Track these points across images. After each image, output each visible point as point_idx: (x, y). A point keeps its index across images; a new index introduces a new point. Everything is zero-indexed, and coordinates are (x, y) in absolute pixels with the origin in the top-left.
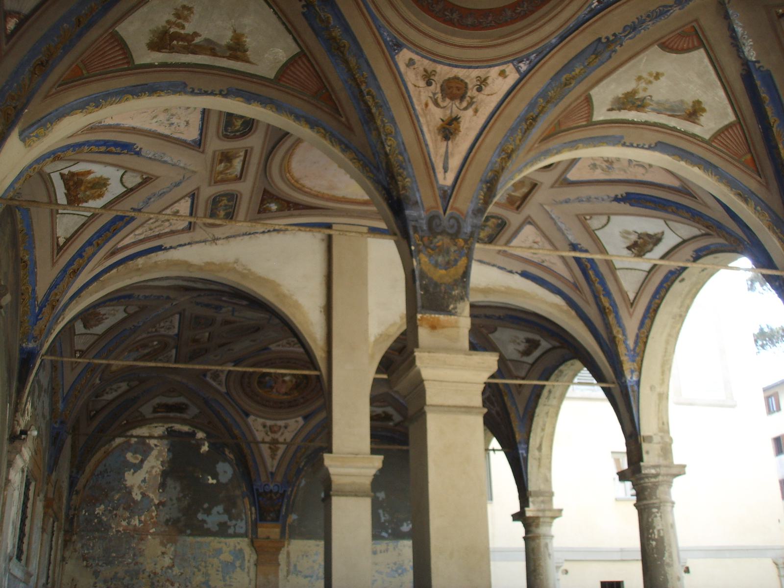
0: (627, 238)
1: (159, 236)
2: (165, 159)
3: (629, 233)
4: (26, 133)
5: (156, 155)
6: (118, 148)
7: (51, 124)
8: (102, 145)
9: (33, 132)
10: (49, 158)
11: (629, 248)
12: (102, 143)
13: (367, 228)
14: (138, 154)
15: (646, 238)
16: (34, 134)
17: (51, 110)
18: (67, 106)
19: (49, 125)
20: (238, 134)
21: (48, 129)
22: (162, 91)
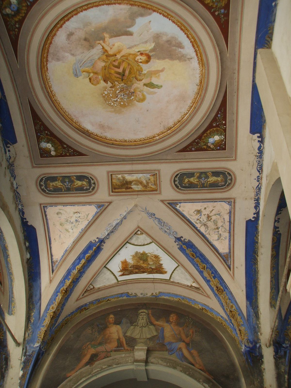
1: (231, 223)
2: (114, 224)
4: (10, 311)
5: (109, 229)
6: (89, 252)
7: (13, 298)
8: (80, 261)
9: (12, 308)
10: (57, 296)
12: (78, 260)
13: (259, 51)
14: (102, 241)
16: (13, 308)
17: (8, 294)
18: (10, 287)
19: (13, 299)
20: (92, 182)
21: (14, 301)
22: (5, 245)
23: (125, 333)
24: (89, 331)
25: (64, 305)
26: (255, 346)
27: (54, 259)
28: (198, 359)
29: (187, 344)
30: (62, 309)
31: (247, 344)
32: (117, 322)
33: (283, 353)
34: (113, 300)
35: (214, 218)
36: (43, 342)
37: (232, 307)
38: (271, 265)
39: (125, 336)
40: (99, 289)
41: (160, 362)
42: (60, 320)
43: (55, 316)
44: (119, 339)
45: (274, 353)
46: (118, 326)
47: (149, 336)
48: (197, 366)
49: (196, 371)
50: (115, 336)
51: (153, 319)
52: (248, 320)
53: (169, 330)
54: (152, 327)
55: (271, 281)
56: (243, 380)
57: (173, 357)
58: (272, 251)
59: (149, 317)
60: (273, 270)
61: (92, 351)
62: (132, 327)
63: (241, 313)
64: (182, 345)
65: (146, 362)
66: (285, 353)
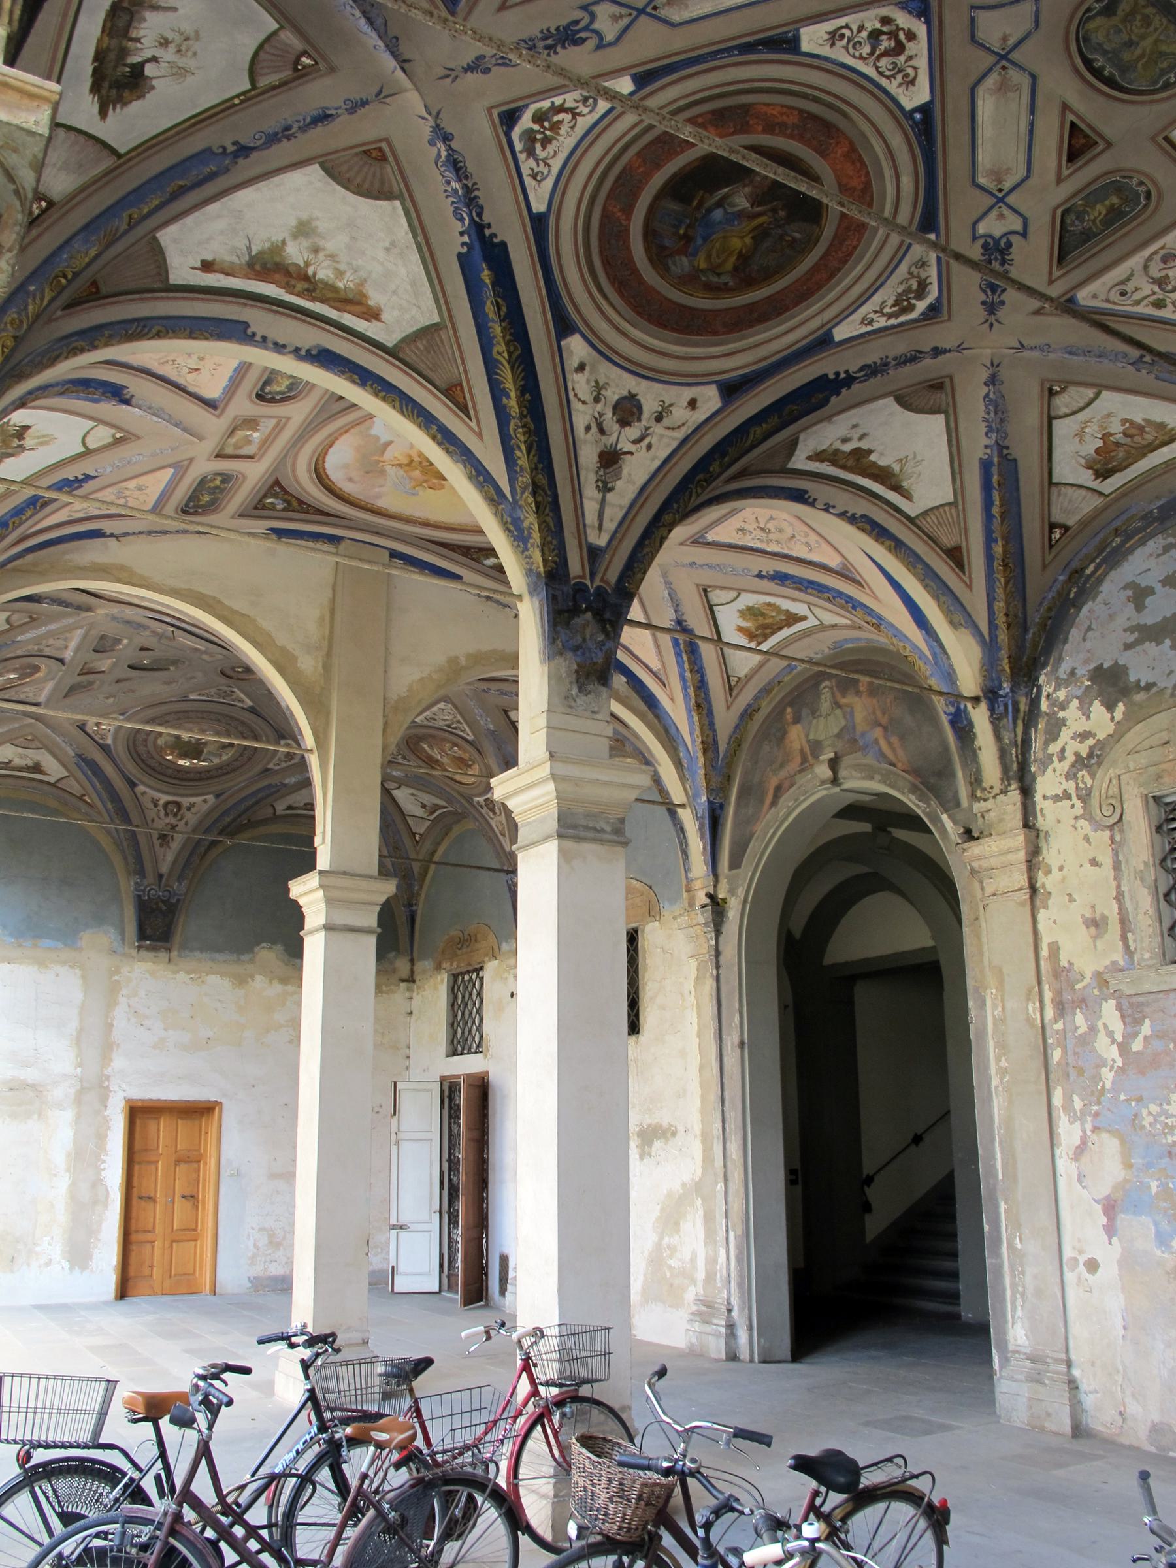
0: (38, 437)
3: (41, 444)
11: (27, 428)
15: (10, 451)
23: (807, 735)
24: (766, 748)
25: (712, 724)
26: (958, 709)
27: (655, 669)
28: (900, 753)
29: (885, 728)
30: (715, 731)
31: (946, 709)
32: (797, 720)
33: (1002, 708)
34: (787, 679)
35: (770, 526)
36: (710, 790)
37: (905, 648)
38: (903, 563)
39: (808, 741)
40: (749, 677)
41: (854, 773)
42: (722, 747)
43: (709, 746)
44: (802, 751)
45: (989, 713)
46: (799, 726)
47: (836, 731)
48: (899, 765)
49: (899, 775)
50: (796, 746)
51: (838, 695)
52: (936, 663)
53: (861, 707)
54: (838, 712)
55: (926, 587)
56: (960, 774)
57: (870, 760)
58: (882, 543)
59: (833, 694)
60: (914, 567)
61: (774, 782)
62: (815, 721)
63: (922, 655)
64: (878, 733)
65: (835, 781)
66: (1006, 705)
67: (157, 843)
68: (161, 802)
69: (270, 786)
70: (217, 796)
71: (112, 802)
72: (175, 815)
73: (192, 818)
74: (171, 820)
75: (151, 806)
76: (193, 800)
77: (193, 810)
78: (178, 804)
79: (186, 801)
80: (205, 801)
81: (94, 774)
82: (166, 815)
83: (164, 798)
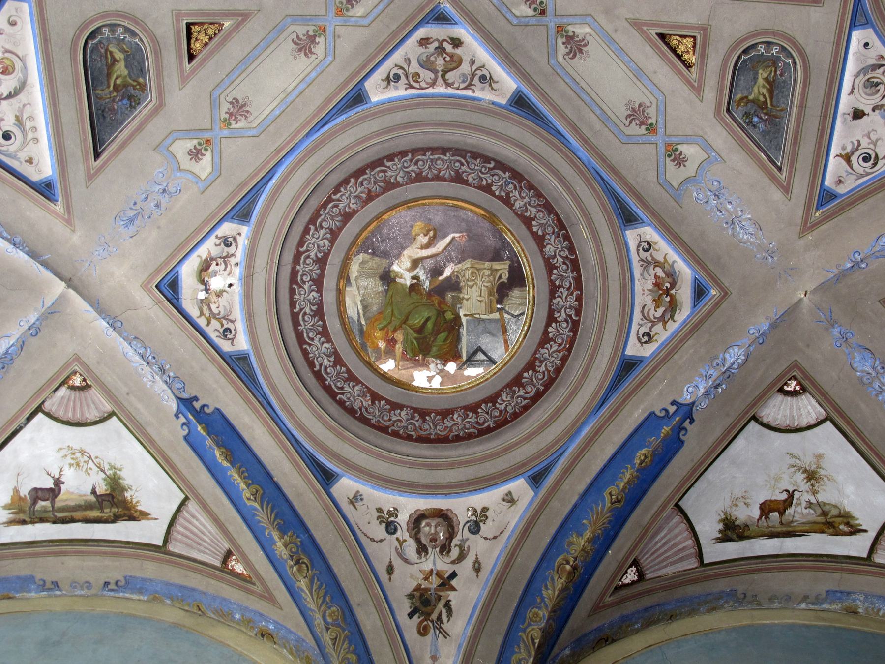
67: (410, 626)
68: (403, 519)
69: (651, 421)
70: (536, 480)
71: (282, 531)
72: (445, 549)
73: (487, 550)
74: (435, 562)
75: (379, 531)
76: (479, 500)
77: (486, 529)
78: (443, 516)
79: (461, 507)
80: (509, 499)
81: (231, 457)
82: (422, 549)
83: (408, 505)
